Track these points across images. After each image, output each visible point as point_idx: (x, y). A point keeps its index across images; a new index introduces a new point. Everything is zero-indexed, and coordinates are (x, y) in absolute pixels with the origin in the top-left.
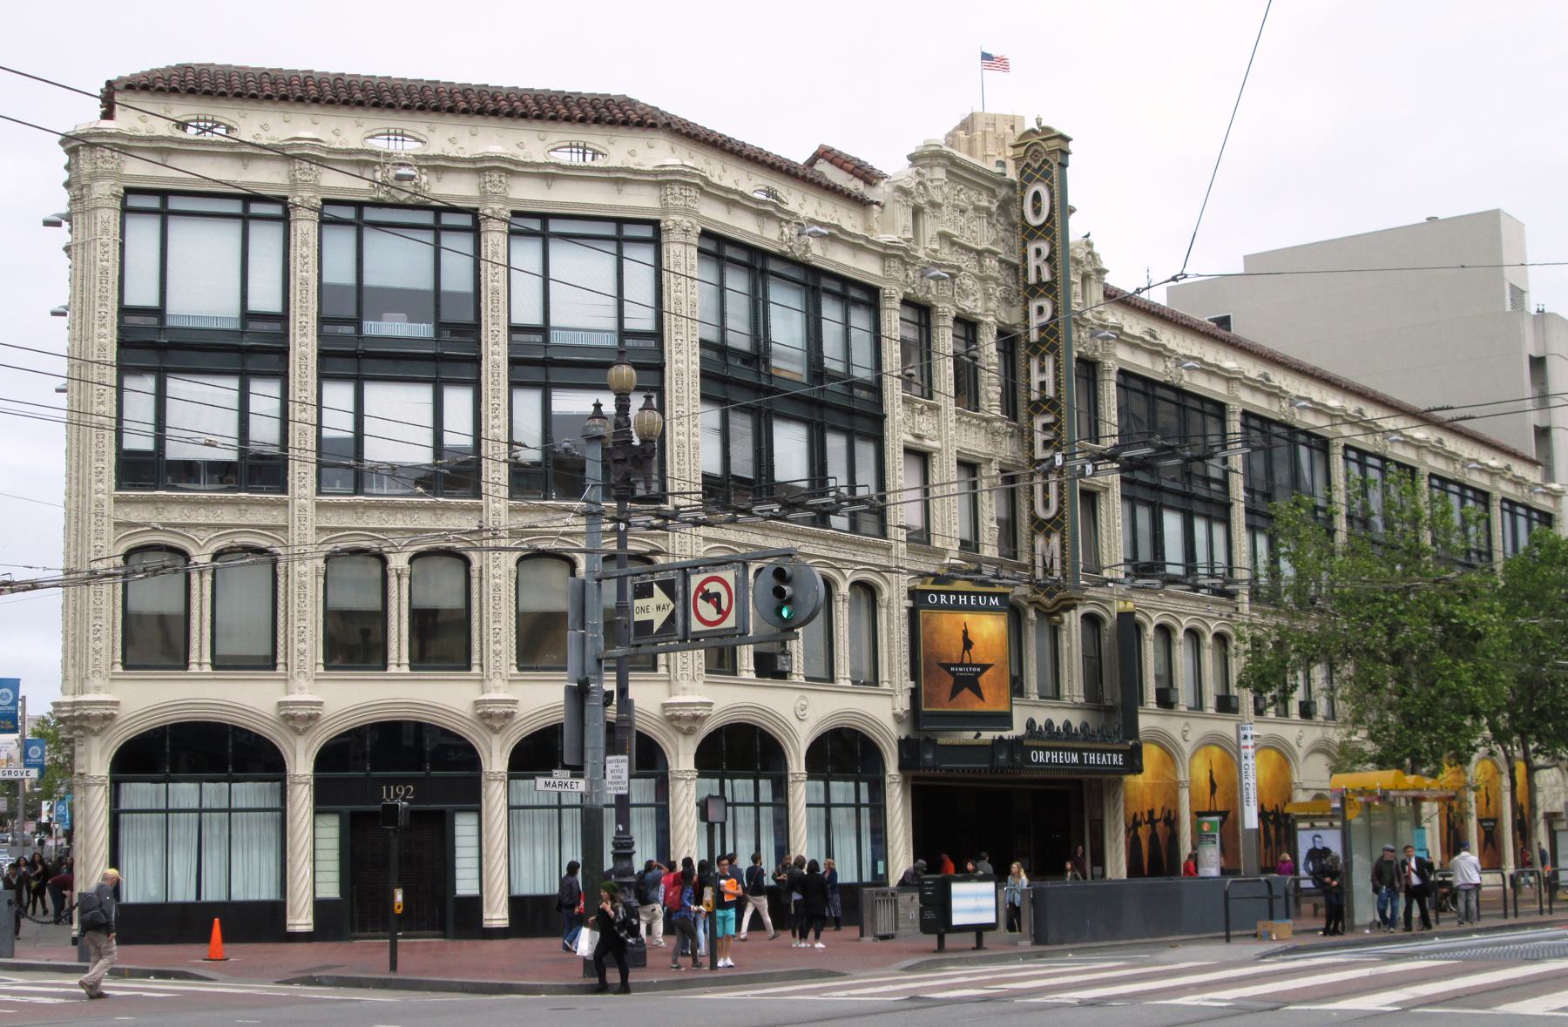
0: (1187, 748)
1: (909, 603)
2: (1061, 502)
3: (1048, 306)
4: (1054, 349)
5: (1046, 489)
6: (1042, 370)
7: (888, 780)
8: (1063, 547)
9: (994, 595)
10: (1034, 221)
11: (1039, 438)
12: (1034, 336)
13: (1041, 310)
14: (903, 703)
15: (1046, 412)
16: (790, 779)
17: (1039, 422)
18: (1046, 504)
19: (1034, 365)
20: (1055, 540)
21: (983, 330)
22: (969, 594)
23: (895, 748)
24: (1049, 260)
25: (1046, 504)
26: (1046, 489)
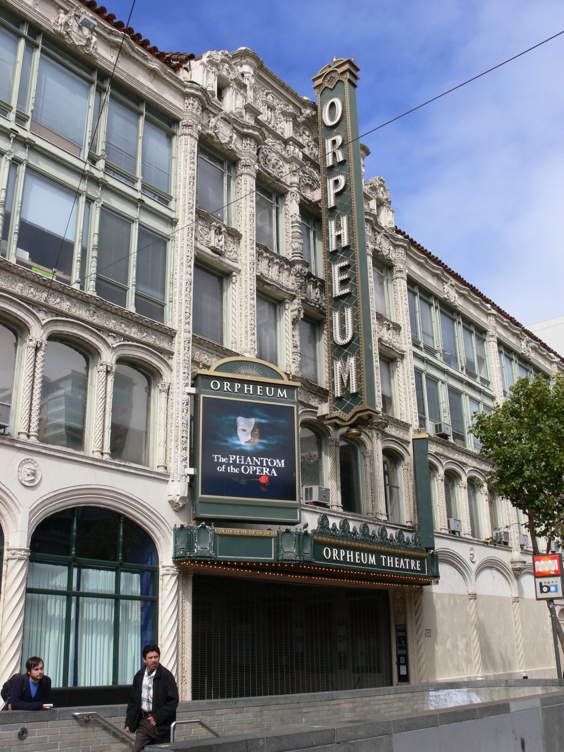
0: (474, 567)
1: (193, 390)
2: (356, 328)
3: (342, 179)
4: (348, 211)
5: (343, 321)
6: (338, 227)
7: (162, 571)
8: (358, 366)
10: (329, 123)
11: (337, 278)
12: (332, 203)
13: (336, 182)
14: (178, 489)
15: (342, 260)
16: (6, 554)
17: (336, 268)
18: (343, 333)
19: (332, 225)
20: (352, 361)
21: (289, 197)
22: (256, 383)
23: (171, 539)
24: (342, 146)
25: (343, 333)
26: (343, 321)
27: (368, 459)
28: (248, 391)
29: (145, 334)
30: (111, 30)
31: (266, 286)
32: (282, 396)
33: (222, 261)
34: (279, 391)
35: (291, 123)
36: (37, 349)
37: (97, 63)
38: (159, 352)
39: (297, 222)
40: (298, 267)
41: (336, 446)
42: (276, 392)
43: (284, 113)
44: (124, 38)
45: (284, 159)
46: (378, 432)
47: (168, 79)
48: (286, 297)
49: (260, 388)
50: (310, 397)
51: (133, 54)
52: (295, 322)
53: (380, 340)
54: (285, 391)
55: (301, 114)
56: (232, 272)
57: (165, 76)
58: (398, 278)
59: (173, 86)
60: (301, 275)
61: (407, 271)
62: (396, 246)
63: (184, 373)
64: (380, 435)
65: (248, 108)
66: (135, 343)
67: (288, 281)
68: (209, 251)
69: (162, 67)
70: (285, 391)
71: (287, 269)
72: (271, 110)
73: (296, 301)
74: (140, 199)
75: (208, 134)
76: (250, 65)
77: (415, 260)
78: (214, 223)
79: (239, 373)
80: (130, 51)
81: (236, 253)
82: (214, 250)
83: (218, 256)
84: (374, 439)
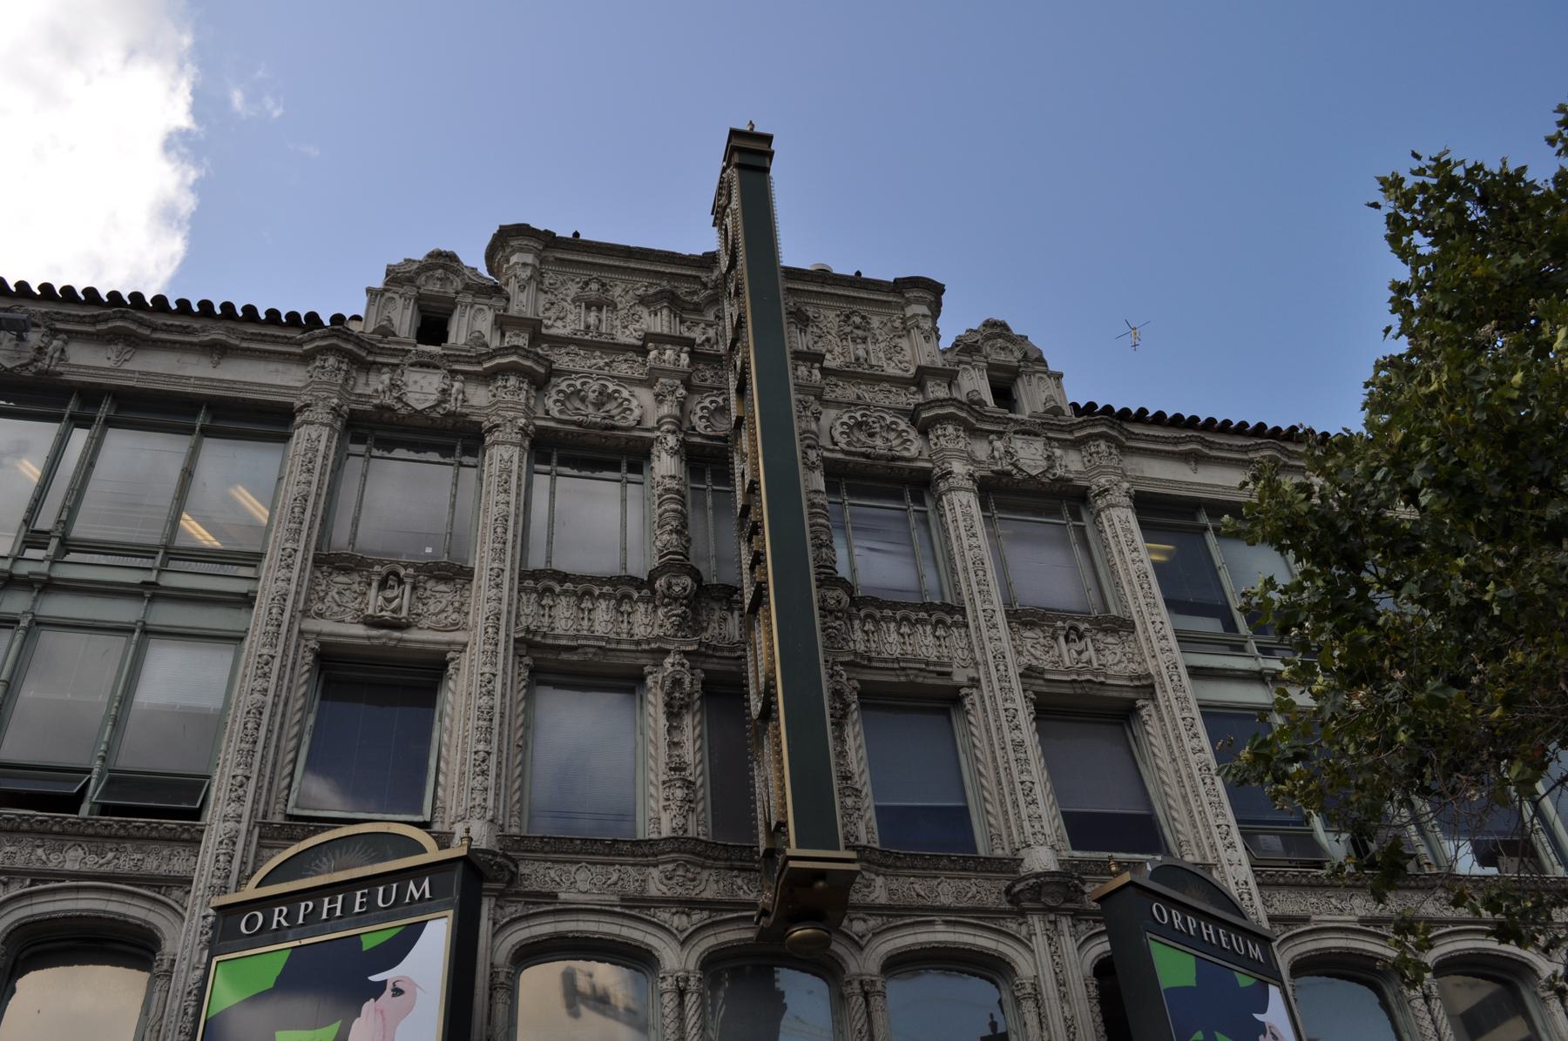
9: (416, 873)
22: (349, 886)
27: (1028, 1005)
28: (331, 911)
29: (110, 855)
30: (93, 316)
31: (565, 656)
32: (417, 896)
33: (400, 640)
34: (412, 886)
35: (665, 312)
36: (682, 993)
37: (69, 382)
38: (149, 887)
39: (667, 490)
40: (660, 583)
41: (866, 995)
42: (401, 892)
43: (643, 301)
44: (123, 318)
45: (640, 383)
46: (1052, 917)
47: (253, 345)
48: (643, 662)
49: (363, 895)
50: (739, 881)
51: (156, 335)
52: (674, 712)
53: (1029, 673)
54: (426, 883)
55: (705, 285)
56: (445, 653)
57: (244, 345)
58: (1102, 510)
59: (275, 352)
60: (676, 599)
61: (1126, 485)
62: (1077, 444)
63: (205, 917)
64: (1065, 924)
65: (503, 323)
66: (68, 883)
67: (645, 623)
68: (360, 630)
69: (229, 331)
70: (426, 883)
71: (641, 599)
72: (600, 309)
73: (669, 660)
74: (144, 583)
75: (376, 406)
76: (521, 250)
77: (1168, 452)
78: (377, 568)
79: (317, 874)
80: (147, 332)
81: (458, 611)
82: (374, 622)
83: (383, 632)
84: (1040, 942)
